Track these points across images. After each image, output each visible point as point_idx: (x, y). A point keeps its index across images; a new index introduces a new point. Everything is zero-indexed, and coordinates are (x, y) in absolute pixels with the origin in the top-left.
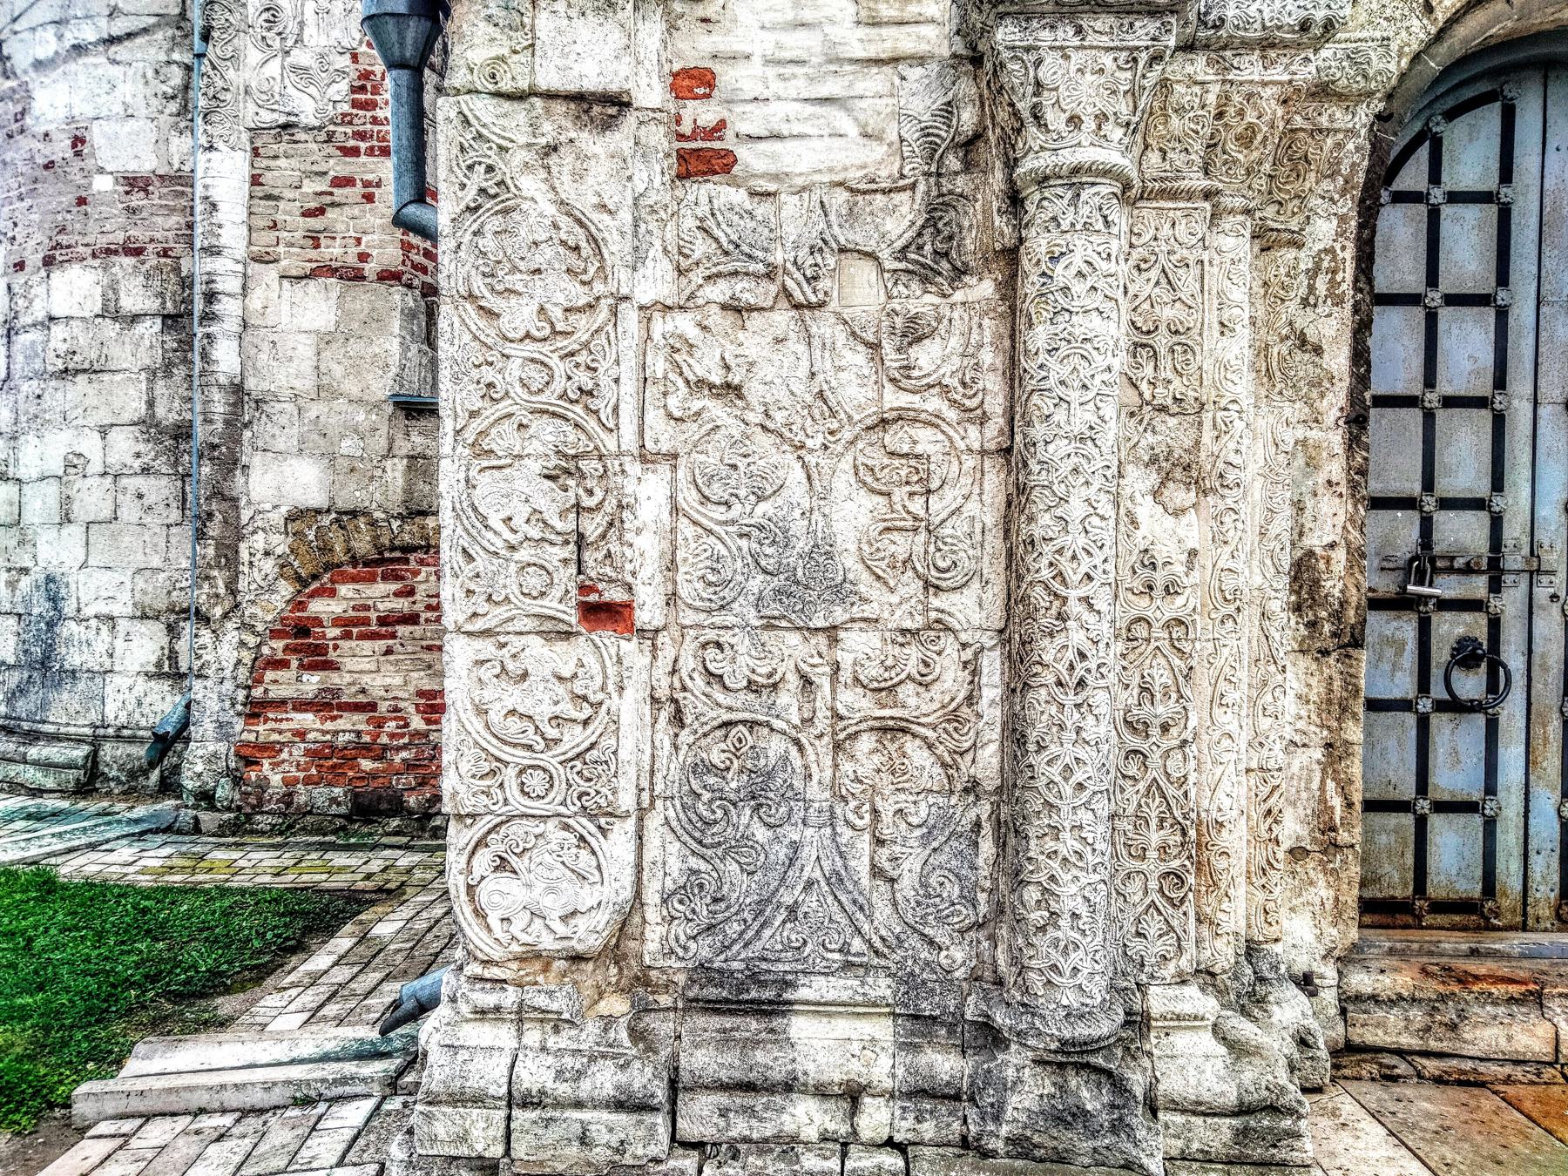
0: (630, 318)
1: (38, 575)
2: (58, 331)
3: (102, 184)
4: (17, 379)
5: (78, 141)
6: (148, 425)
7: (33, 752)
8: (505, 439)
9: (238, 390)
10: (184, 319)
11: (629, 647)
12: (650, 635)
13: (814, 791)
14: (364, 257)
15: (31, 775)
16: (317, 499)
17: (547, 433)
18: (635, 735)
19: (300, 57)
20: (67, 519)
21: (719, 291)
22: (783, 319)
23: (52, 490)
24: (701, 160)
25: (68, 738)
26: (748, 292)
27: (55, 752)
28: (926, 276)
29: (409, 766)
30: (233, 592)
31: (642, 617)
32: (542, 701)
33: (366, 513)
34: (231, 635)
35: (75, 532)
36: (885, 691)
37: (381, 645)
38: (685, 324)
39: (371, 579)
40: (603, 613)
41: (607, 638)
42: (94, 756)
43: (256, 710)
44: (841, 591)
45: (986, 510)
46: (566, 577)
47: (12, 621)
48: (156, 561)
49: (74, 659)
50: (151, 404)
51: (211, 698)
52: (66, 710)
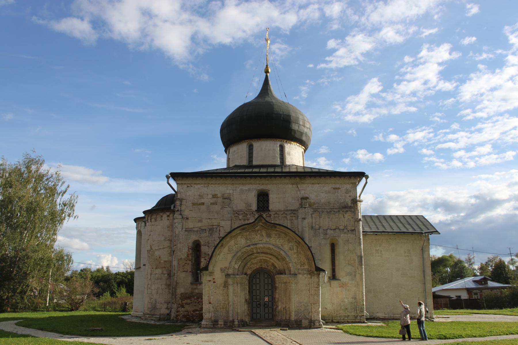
3: (162, 261)
6: (166, 284)
9: (176, 282)
10: (169, 275)
15: (154, 319)
16: (183, 292)
18: (211, 309)
24: (214, 282)
40: (210, 303)
43: (177, 312)
49: (158, 307)
51: (173, 311)
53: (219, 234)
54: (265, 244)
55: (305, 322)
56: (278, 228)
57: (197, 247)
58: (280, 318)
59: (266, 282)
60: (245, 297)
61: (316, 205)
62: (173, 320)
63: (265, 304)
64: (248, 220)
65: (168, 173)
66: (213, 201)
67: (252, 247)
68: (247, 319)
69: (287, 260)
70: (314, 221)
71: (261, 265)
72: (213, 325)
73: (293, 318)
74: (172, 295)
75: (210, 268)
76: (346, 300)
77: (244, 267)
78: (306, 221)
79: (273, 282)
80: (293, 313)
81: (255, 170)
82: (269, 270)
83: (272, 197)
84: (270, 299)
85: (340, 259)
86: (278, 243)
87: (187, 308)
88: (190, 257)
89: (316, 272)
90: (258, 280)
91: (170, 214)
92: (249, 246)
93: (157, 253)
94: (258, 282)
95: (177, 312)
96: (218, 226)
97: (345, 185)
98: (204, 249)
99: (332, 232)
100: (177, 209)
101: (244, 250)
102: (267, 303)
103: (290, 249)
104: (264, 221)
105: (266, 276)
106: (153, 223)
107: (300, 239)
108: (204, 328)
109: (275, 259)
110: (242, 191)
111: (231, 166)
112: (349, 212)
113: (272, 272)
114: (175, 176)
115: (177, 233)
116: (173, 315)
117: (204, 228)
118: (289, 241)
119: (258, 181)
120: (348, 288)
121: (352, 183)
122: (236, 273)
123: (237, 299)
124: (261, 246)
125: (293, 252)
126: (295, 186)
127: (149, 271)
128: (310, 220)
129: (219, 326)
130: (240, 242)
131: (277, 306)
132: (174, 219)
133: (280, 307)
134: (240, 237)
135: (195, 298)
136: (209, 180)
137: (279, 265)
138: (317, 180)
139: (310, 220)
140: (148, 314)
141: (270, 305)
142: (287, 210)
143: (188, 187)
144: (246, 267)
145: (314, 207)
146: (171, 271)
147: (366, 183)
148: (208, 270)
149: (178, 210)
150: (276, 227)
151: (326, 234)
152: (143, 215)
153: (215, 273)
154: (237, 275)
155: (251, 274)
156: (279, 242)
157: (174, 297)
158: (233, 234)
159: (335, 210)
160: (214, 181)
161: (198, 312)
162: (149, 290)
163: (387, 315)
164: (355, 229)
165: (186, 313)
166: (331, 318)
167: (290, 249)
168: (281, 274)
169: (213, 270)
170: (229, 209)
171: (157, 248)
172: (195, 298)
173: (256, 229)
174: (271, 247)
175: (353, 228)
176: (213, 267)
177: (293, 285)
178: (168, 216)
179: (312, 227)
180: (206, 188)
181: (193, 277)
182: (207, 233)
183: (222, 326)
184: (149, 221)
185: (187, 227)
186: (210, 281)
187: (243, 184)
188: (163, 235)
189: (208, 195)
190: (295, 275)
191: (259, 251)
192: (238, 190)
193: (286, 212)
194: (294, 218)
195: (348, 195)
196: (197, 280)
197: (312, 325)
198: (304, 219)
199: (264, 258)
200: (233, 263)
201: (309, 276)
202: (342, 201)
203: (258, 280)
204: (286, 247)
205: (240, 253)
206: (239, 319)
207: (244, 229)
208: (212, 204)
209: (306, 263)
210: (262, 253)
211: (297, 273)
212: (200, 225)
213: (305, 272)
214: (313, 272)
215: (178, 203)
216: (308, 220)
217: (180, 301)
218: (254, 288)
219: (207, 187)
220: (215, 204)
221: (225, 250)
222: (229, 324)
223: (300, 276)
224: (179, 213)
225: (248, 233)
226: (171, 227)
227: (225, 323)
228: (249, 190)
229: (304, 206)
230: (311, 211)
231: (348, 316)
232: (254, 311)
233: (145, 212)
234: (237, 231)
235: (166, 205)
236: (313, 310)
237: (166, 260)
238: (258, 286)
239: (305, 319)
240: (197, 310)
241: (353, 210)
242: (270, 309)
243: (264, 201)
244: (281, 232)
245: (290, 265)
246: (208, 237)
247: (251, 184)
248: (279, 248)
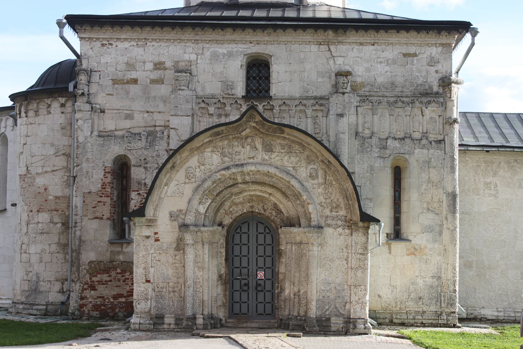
0: (150, 255)
1: (34, 273)
2: (40, 225)
3: (51, 197)
4: (29, 233)
5: (45, 189)
6: (58, 243)
7: (35, 307)
8: (139, 266)
10: (66, 225)
11: (150, 284)
12: (152, 283)
13: (167, 297)
14: (103, 215)
15: (35, 312)
16: (94, 259)
17: (143, 265)
19: (92, 180)
20: (41, 262)
21: (158, 252)
22: (164, 254)
23: (38, 256)
24: (157, 240)
25: (41, 305)
26: (161, 252)
27: (39, 307)
28: (177, 250)
29: (110, 308)
30: (79, 276)
31: (151, 281)
32: (142, 289)
33: (103, 262)
34: (78, 284)
35: (43, 264)
36: (174, 288)
37: (105, 286)
38: (155, 255)
39: (104, 273)
40: (148, 281)
41: (148, 283)
42: (46, 308)
43: (82, 298)
44: (169, 279)
45: (182, 272)
46: (144, 278)
47: (27, 282)
48: (60, 270)
49: (42, 289)
50: (59, 240)
51: (74, 296)
52: (41, 300)
53: (168, 144)
54: (261, 164)
55: (337, 322)
56: (288, 134)
57: (121, 169)
58: (287, 313)
59: (261, 240)
60: (219, 271)
61: (367, 89)
62: (73, 314)
63: (258, 285)
64: (226, 115)
65: (61, 16)
66: (154, 75)
67: (234, 170)
68: (221, 314)
69: (305, 197)
70: (361, 121)
71: (252, 207)
72: (154, 324)
73: (313, 312)
74: (72, 265)
75: (149, 211)
76: (420, 281)
77: (218, 210)
78: (345, 120)
79: (275, 241)
80: (314, 303)
81: (243, 13)
82: (268, 217)
83: (278, 71)
84: (269, 276)
85: (412, 199)
86: (286, 163)
87: (102, 290)
88: (109, 190)
89: (361, 224)
90: (244, 238)
91: (66, 101)
92: (228, 168)
93: (40, 181)
94: (244, 240)
95: (82, 298)
96: (166, 127)
97: (427, 48)
98: (137, 173)
99: (397, 144)
100: (80, 92)
101: (218, 176)
102: (262, 283)
103: (311, 176)
104: (258, 118)
105: (261, 229)
106: (31, 120)
107: (331, 156)
108: (135, 330)
109: (279, 195)
110: (215, 57)
111: (193, 3)
112: (433, 104)
113: (273, 221)
114: (76, 22)
115: (81, 139)
116: (73, 304)
117: (136, 131)
118: (309, 161)
119: (249, 35)
120: (425, 257)
121: (442, 45)
122: (201, 222)
123: (203, 273)
124: (253, 168)
125: (316, 181)
126: (324, 48)
127: (25, 217)
128: (353, 119)
129: (165, 326)
130: (209, 161)
131: (282, 290)
132: (74, 111)
133: (287, 292)
134: (210, 149)
135: (119, 271)
136: (146, 33)
137: (287, 207)
138: (370, 36)
139: (353, 119)
140: (22, 303)
141: (268, 287)
142: (307, 98)
143: (103, 45)
144: (222, 211)
145: (361, 92)
146: (68, 217)
147: (473, 44)
148: (143, 215)
149: (83, 94)
150: (283, 132)
151: (385, 148)
152: (10, 103)
153: (159, 222)
154: (203, 226)
155: (232, 224)
156: (288, 161)
157: (74, 269)
158: (196, 143)
159: (405, 99)
160: (157, 33)
161: (123, 300)
162: (24, 255)
163: (501, 314)
164: (444, 140)
165: (99, 301)
166: (388, 316)
167: (311, 176)
168: (292, 225)
169: (154, 215)
170: (187, 93)
171: (40, 170)
172: (119, 271)
173: (244, 133)
174: (272, 170)
175: (440, 138)
176: (155, 210)
177: (315, 248)
178: (63, 105)
179: (357, 134)
180: (142, 49)
181: (114, 229)
182: (144, 140)
183: (172, 326)
184: (23, 114)
185: (101, 129)
186: (148, 237)
187: (217, 42)
188: (52, 145)
189: (144, 62)
190: (320, 227)
191: (247, 178)
192: (207, 54)
193: (304, 102)
194: (320, 114)
195: (433, 69)
196: (121, 235)
197: (349, 327)
198: (341, 115)
199: (258, 193)
200: (195, 202)
201: (347, 231)
202: (420, 82)
203: (244, 238)
204: (303, 172)
205: (208, 184)
206: (206, 313)
207: (218, 134)
208: (153, 81)
209: (342, 205)
210: (254, 183)
211: (323, 224)
212: (127, 124)
213: (340, 223)
214: (356, 224)
215: (83, 78)
216: (350, 119)
217: (88, 276)
218: (237, 251)
219: (143, 46)
220: (160, 81)
221: (180, 175)
222: (185, 323)
223: (328, 231)
224: (85, 99)
225: (226, 142)
226: (68, 127)
227: (178, 321)
228: (230, 55)
229: (341, 91)
230: (355, 100)
231: (424, 312)
232: (237, 298)
233: (13, 97)
234: (205, 138)
235: (58, 83)
236: (354, 298)
237: (59, 194)
238: (245, 249)
239: (336, 315)
240: (121, 296)
241: (441, 100)
242: (268, 295)
243: (260, 78)
244: (293, 141)
245: (311, 208)
246: (146, 149)
247: (234, 41)
248: (288, 173)
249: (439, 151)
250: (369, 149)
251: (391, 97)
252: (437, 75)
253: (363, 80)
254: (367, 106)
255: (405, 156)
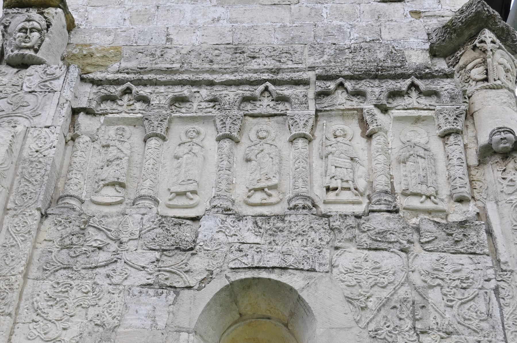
112: (413, 100)
159: (287, 91)
241: (445, 86)
249: (465, 259)
250: (103, 257)
251: (228, 84)
252: (418, 23)
253: (120, 42)
254: (125, 109)
255: (285, 278)
